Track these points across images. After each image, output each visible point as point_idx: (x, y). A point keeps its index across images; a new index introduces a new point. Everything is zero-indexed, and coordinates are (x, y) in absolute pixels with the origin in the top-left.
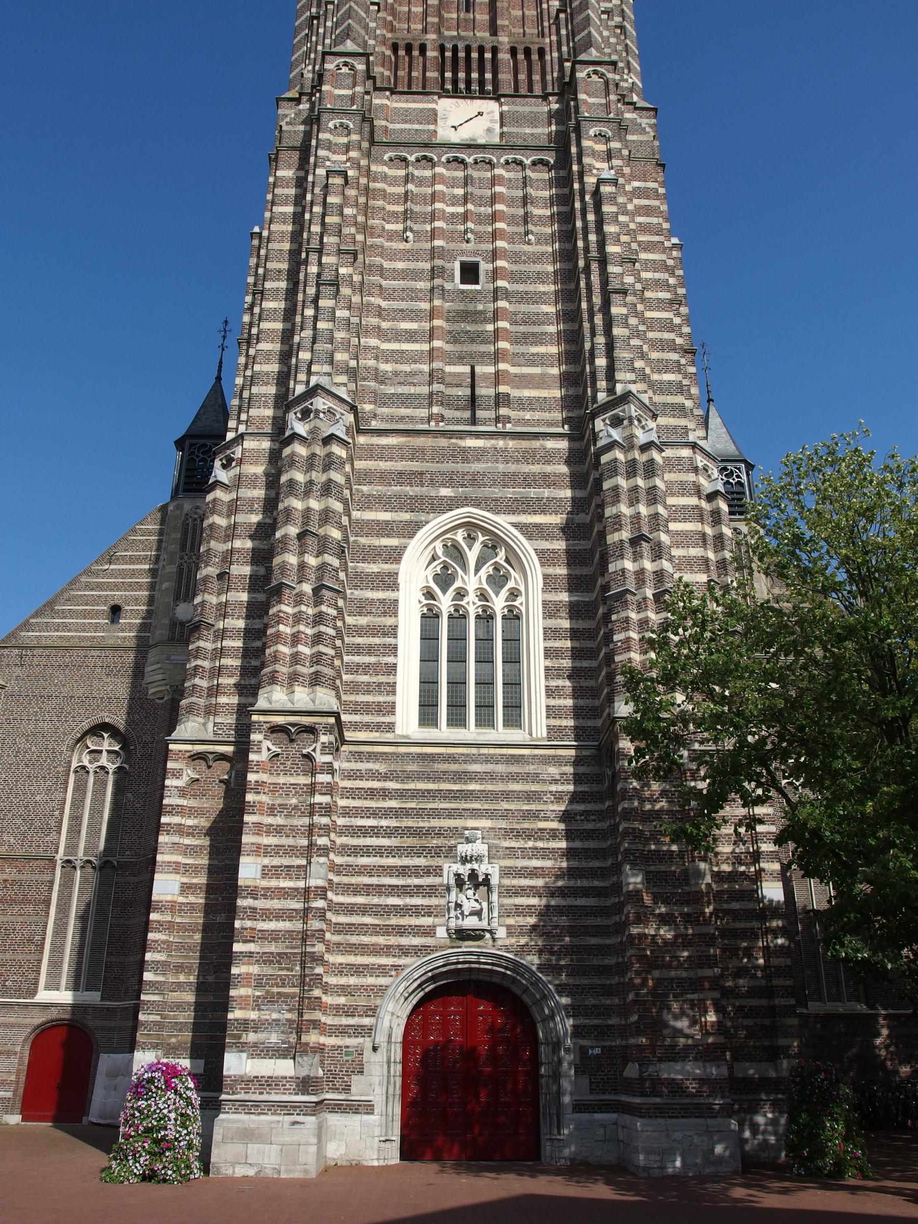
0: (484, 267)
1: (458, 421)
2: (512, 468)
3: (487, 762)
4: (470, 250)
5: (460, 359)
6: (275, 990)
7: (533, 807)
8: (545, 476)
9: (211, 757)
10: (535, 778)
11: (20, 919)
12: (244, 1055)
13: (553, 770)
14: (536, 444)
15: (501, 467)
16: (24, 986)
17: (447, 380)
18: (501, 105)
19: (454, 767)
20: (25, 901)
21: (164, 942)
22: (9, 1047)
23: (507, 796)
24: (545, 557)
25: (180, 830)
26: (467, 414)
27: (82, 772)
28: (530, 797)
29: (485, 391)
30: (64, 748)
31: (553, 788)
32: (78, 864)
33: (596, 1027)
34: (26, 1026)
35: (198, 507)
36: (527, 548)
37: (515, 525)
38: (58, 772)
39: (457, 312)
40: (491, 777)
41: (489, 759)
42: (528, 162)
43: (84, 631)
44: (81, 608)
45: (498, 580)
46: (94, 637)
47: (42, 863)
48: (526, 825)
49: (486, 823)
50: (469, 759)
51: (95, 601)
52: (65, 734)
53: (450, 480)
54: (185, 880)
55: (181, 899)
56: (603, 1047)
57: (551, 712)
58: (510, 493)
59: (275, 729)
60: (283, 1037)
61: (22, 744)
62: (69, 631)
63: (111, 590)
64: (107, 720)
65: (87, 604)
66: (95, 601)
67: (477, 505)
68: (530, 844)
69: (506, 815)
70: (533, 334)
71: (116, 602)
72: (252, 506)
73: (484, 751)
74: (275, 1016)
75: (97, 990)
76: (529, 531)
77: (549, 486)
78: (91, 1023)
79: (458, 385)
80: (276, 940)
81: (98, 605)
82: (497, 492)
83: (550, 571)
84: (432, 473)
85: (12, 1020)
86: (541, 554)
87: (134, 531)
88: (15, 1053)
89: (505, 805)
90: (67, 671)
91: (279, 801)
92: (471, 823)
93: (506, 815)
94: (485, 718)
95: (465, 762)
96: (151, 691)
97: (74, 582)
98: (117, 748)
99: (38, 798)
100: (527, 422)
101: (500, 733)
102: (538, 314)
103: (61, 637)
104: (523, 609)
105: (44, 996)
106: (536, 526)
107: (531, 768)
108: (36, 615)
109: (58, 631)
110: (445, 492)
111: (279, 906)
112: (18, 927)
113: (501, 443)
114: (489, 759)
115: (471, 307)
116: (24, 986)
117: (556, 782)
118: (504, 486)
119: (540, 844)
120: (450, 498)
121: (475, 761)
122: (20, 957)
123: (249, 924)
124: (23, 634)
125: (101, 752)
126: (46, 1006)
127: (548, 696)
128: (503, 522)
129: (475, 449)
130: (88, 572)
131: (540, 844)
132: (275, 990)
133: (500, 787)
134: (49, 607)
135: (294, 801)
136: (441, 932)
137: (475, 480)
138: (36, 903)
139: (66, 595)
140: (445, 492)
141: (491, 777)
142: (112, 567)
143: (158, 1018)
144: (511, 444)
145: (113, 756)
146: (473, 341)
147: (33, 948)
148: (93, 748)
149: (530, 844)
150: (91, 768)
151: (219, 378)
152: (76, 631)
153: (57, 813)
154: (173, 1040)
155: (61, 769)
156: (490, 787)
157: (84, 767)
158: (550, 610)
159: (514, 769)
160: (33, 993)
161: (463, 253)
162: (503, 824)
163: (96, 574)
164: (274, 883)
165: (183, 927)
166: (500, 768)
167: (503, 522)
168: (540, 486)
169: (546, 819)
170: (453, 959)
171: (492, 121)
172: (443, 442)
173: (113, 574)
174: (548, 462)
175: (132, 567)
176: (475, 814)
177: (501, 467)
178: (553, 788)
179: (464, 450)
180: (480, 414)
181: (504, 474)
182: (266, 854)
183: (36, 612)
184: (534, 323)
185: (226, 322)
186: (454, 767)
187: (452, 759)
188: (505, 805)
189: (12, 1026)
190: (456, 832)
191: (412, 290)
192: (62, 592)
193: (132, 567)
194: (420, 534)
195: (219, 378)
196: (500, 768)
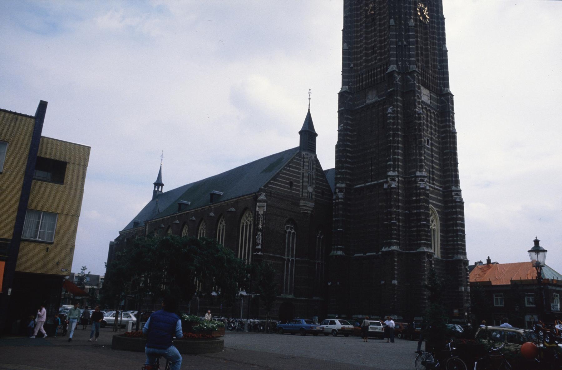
0: (430, 141)
128: (435, 209)
151: (309, 110)
173: (289, 170)
195: (309, 110)
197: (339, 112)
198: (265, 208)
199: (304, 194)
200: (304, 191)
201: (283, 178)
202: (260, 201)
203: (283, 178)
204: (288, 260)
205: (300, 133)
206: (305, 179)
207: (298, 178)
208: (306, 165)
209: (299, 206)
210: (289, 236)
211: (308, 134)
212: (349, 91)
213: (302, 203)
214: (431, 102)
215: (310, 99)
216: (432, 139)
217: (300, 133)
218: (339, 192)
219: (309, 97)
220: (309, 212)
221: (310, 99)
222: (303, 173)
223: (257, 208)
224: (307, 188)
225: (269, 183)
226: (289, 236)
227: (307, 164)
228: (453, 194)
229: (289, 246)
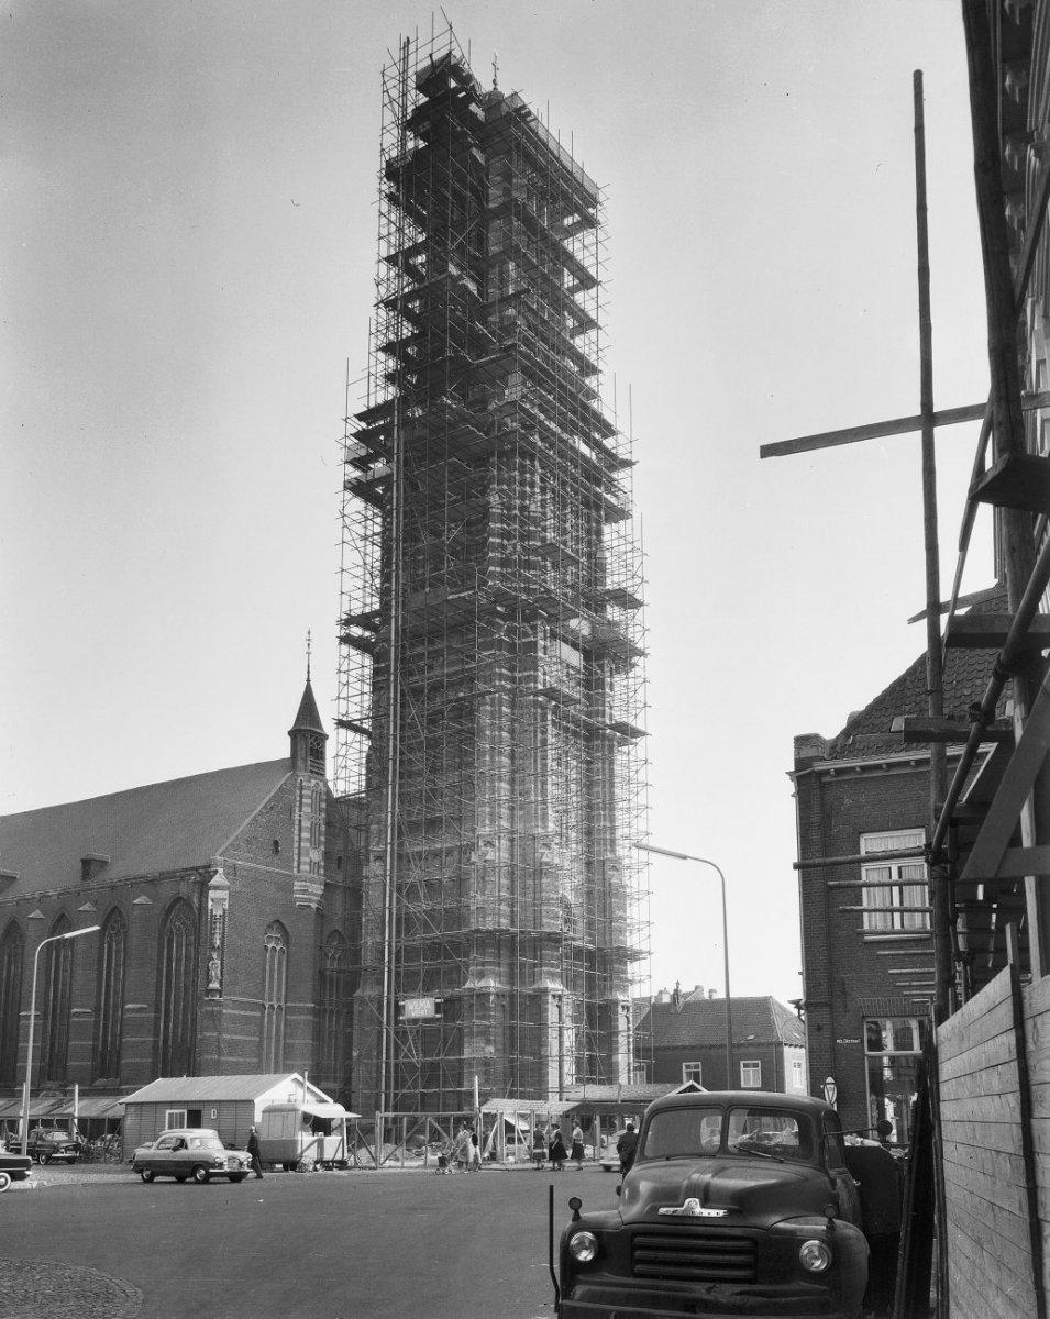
151: (308, 681)
185: (309, 633)
195: (308, 681)
198: (227, 903)
199: (302, 867)
200: (303, 859)
202: (216, 888)
204: (272, 1006)
205: (290, 733)
206: (305, 835)
208: (307, 805)
209: (292, 892)
210: (272, 958)
211: (307, 736)
213: (297, 885)
215: (308, 653)
217: (290, 733)
219: (307, 650)
220: (314, 905)
221: (308, 653)
222: (300, 821)
223: (210, 903)
224: (308, 855)
226: (272, 958)
227: (309, 801)
229: (272, 977)
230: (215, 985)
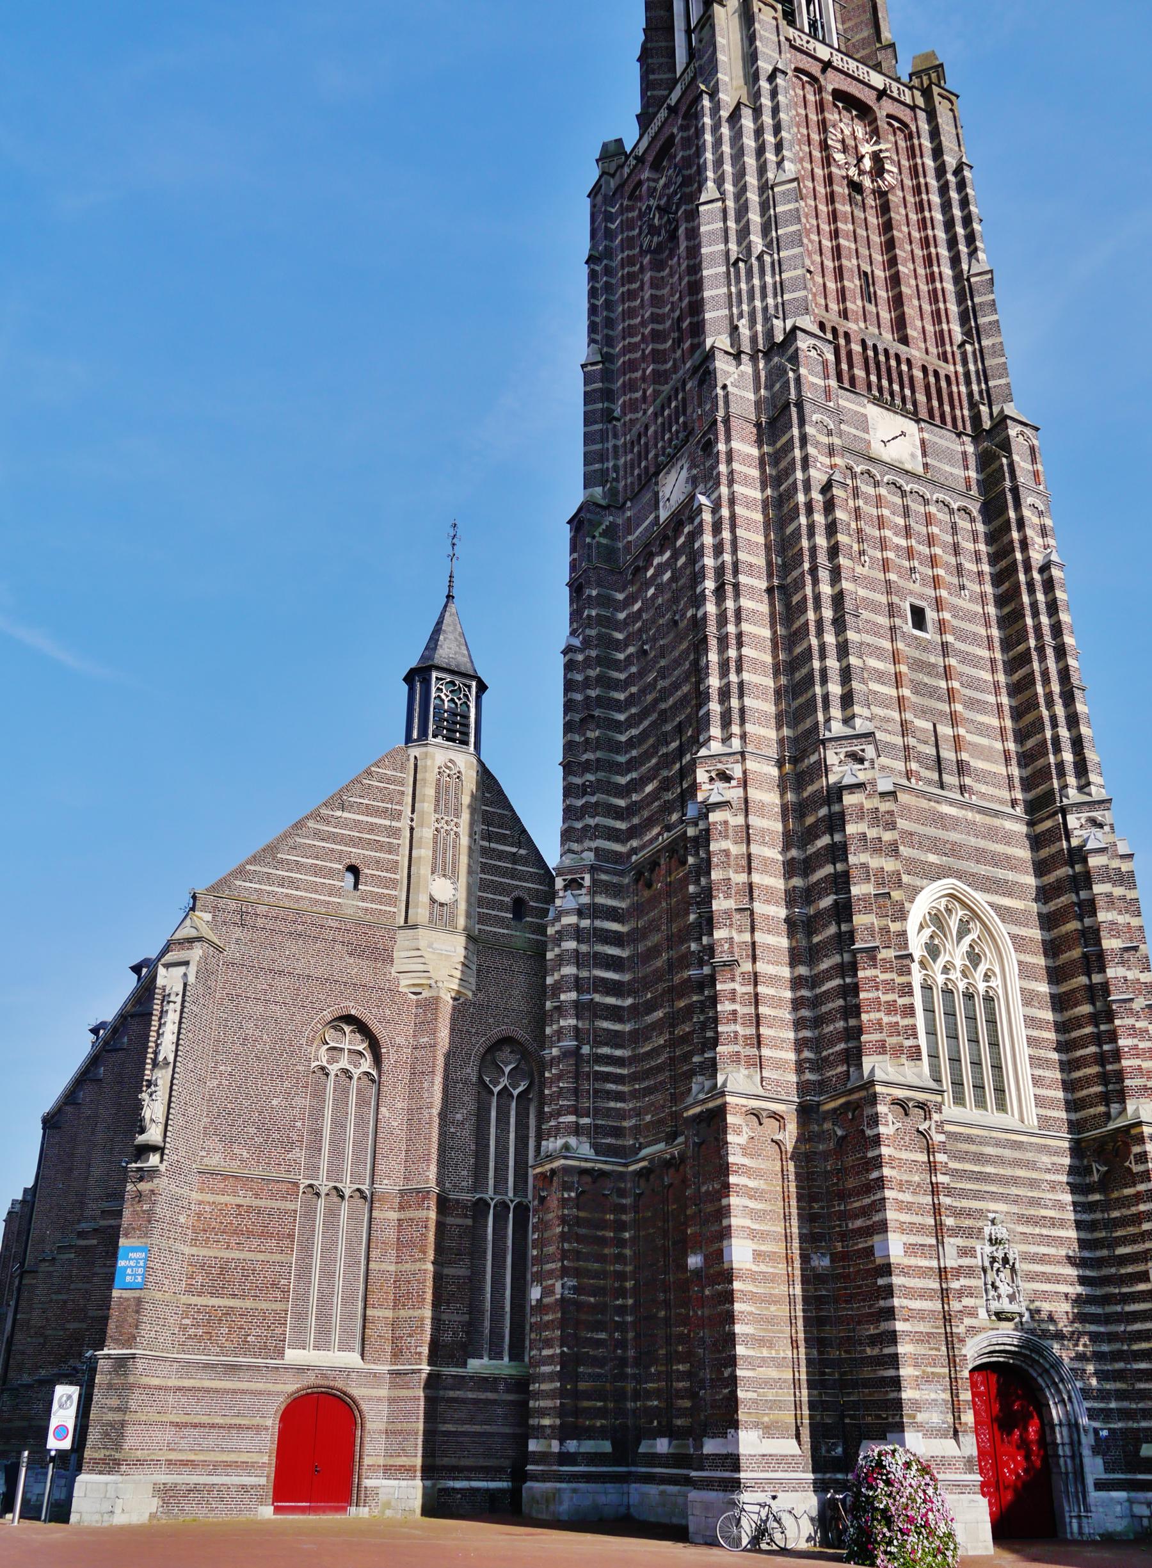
0: (931, 615)
1: (929, 782)
2: (982, 843)
3: (997, 1145)
4: (917, 592)
5: (923, 712)
6: (929, 1370)
7: (1035, 1194)
8: (1008, 858)
9: (764, 1114)
10: (1030, 1165)
11: (261, 1257)
12: (920, 1435)
13: (1046, 1160)
14: (997, 822)
15: (973, 841)
16: (271, 1343)
17: (918, 734)
18: (921, 430)
19: (973, 1148)
20: (265, 1234)
21: (751, 1313)
22: (257, 1421)
23: (1015, 1181)
24: (1019, 943)
25: (753, 1194)
26: (936, 776)
27: (319, 1074)
28: (1033, 1184)
29: (948, 754)
30: (303, 1041)
31: (1048, 1177)
32: (323, 1191)
33: (1102, 1410)
34: (278, 1394)
35: (451, 761)
36: (1003, 930)
37: (991, 905)
38: (298, 1072)
39: (915, 660)
40: (1000, 1161)
41: (998, 1144)
42: (955, 506)
43: (316, 892)
44: (310, 861)
45: (974, 958)
46: (328, 903)
47: (284, 1187)
48: (1032, 1212)
49: (1001, 1207)
50: (983, 1142)
51: (329, 854)
52: (303, 1024)
53: (935, 846)
54: (755, 1247)
55: (755, 1268)
56: (1109, 1429)
57: (1040, 1101)
58: (983, 870)
59: (901, 1104)
60: (942, 1416)
61: (250, 1028)
62: (297, 889)
63: (346, 845)
64: (353, 1012)
65: (317, 858)
66: (329, 854)
67: (959, 878)
68: (1037, 1231)
69: (1017, 1200)
70: (978, 701)
71: (354, 862)
72: (763, 837)
73: (994, 1134)
74: (933, 1396)
75: (352, 1350)
76: (1005, 913)
77: (1011, 869)
78: (355, 1392)
79: (926, 743)
80: (923, 1318)
81: (331, 861)
82: (971, 867)
83: (1023, 957)
84: (920, 836)
85: (260, 1386)
86: (1013, 937)
87: (369, 773)
88: (266, 1428)
89: (1014, 1191)
90: (300, 942)
91: (905, 1177)
92: (992, 1206)
93: (1017, 1200)
94: (981, 1103)
95: (981, 1143)
96: (403, 983)
97: (299, 825)
98: (360, 1048)
99: (275, 1102)
100: (983, 796)
101: (992, 1117)
102: (979, 679)
103: (287, 895)
104: (1000, 992)
105: (293, 1356)
106: (1007, 909)
107: (1029, 1156)
108: (254, 860)
109: (283, 886)
110: (932, 858)
111: (920, 1285)
112: (258, 1267)
113: (970, 815)
114: (998, 1144)
115: (924, 657)
116: (271, 1343)
117: (1048, 1171)
118: (978, 862)
119: (1045, 1232)
120: (939, 866)
121: (988, 1144)
122: (264, 1305)
123: (906, 1302)
124: (238, 883)
125: (342, 1050)
126: (301, 1370)
127: (1035, 1085)
128: (981, 899)
129: (952, 817)
130: (315, 815)
131: (1045, 1232)
132: (929, 1370)
133: (1008, 1172)
134: (269, 853)
135: (916, 1178)
136: (983, 1314)
137: (954, 850)
138: (280, 1237)
139: (291, 842)
140: (932, 858)
141: (1000, 1161)
142: (346, 815)
143: (754, 1395)
144: (978, 818)
145: (356, 1057)
146: (931, 696)
147: (279, 1295)
148: (332, 1044)
149: (1037, 1231)
150: (333, 1069)
152: (306, 890)
153: (299, 1124)
154: (766, 1419)
155: (301, 1068)
156: (1002, 1172)
157: (323, 1068)
158: (1028, 998)
159: (1017, 1154)
160: (281, 1354)
161: (911, 593)
162: (1015, 1209)
163: (326, 820)
164: (913, 1261)
165: (770, 1300)
166: (1007, 1153)
167: (981, 899)
168: (1004, 868)
169: (1046, 1207)
170: (994, 1341)
171: (914, 445)
172: (924, 804)
174: (1008, 844)
175: (370, 819)
176: (995, 1197)
177: (973, 841)
178: (1048, 1177)
179: (943, 816)
180: (946, 778)
181: (977, 849)
182: (910, 1232)
183: (254, 857)
184: (976, 689)
186: (973, 1148)
187: (969, 1139)
188: (1014, 1191)
189: (260, 1393)
190: (980, 1214)
191: (875, 624)
192: (286, 836)
193: (370, 819)
194: (919, 898)
196: (1007, 1153)
197: (570, 585)
201: (305, 850)
203: (305, 850)
207: (391, 849)
212: (603, 502)
214: (926, 465)
215: (452, 557)
216: (939, 604)
218: (566, 888)
221: (452, 557)
225: (240, 872)
228: (1072, 821)
230: (153, 1135)
